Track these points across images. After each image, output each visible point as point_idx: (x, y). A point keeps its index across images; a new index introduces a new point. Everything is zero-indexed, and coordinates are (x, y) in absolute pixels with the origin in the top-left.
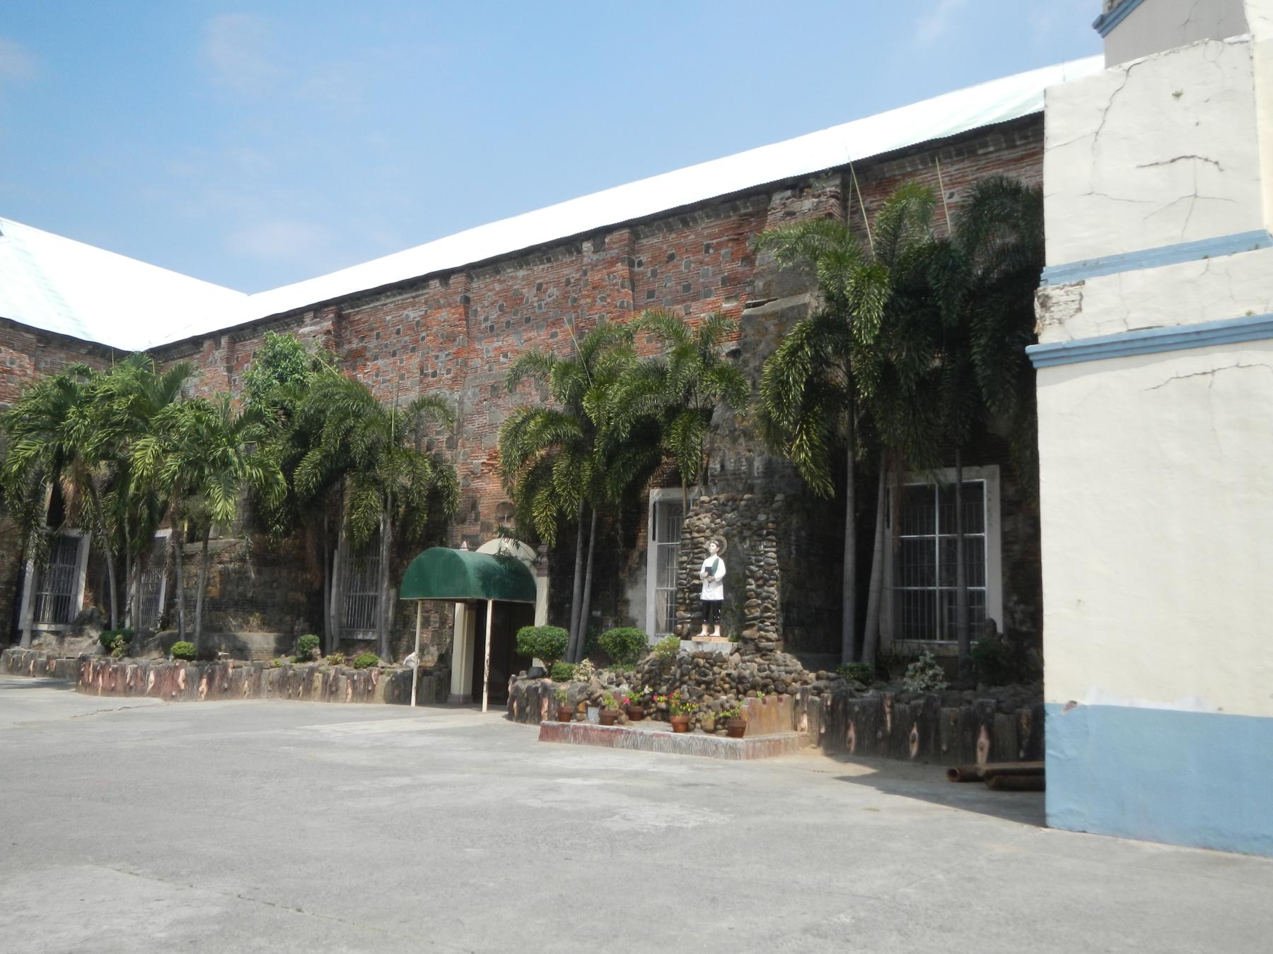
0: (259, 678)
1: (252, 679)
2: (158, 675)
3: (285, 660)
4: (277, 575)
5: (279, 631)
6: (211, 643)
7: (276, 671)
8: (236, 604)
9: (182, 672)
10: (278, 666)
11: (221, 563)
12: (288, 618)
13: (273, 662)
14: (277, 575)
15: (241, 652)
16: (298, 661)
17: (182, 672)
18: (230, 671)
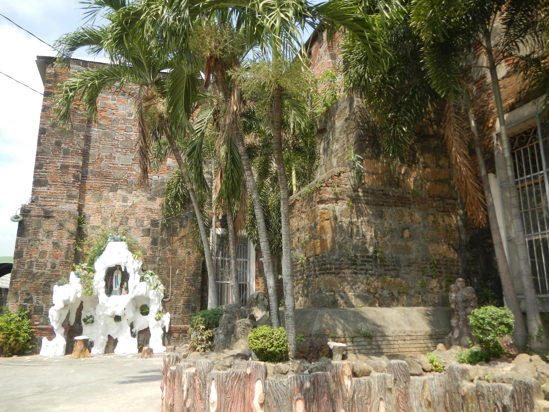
0: (406, 396)
1: (392, 397)
2: (221, 391)
3: (452, 357)
4: (407, 219)
5: (424, 303)
6: (316, 327)
7: (434, 382)
8: (354, 262)
9: (258, 387)
10: (436, 369)
11: (322, 202)
12: (434, 283)
13: (425, 360)
14: (407, 219)
15: (370, 341)
16: (475, 359)
17: (258, 387)
18: (347, 382)
